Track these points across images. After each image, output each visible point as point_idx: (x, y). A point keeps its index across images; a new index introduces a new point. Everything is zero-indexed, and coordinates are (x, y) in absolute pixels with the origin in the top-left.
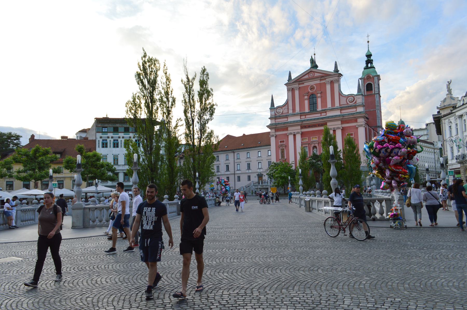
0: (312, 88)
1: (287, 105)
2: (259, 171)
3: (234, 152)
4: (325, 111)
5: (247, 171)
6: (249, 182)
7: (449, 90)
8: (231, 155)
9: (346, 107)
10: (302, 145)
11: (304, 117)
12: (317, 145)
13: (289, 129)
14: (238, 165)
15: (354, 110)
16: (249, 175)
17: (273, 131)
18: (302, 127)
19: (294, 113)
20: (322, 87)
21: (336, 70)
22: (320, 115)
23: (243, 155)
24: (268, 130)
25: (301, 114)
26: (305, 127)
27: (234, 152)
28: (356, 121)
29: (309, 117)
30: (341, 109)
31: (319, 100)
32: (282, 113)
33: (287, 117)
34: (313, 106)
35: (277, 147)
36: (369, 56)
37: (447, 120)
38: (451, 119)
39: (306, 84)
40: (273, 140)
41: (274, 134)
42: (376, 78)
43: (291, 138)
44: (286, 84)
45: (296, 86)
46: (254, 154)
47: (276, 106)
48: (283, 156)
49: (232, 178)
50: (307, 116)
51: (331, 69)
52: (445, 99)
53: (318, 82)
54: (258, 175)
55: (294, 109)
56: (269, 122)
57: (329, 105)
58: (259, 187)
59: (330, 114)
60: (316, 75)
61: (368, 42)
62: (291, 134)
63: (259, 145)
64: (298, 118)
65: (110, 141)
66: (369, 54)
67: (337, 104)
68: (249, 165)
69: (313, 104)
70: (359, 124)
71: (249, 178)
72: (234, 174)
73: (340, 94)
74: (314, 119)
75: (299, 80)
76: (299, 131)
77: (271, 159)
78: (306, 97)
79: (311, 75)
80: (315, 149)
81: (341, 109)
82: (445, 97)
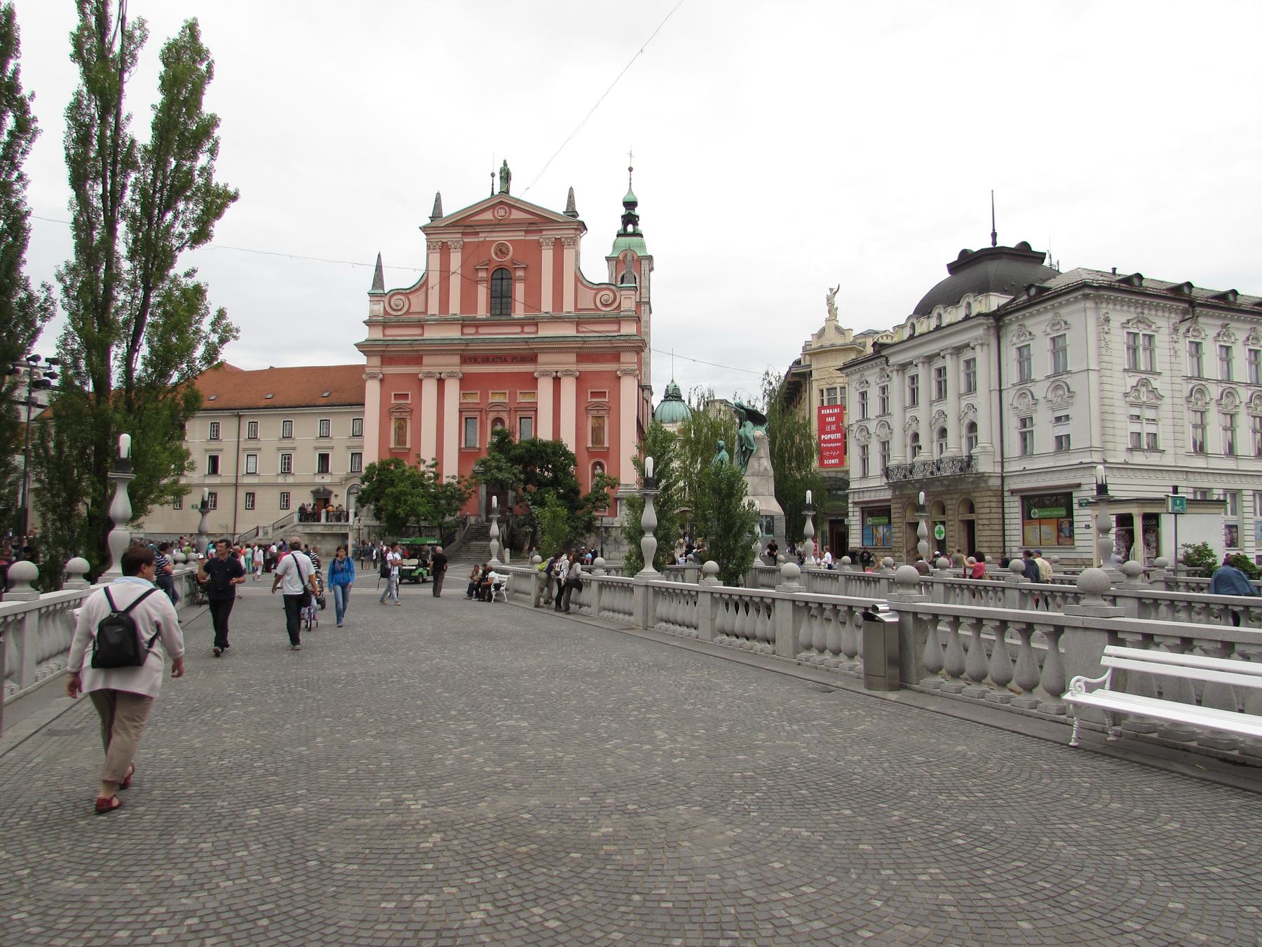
0: (502, 251)
2: (318, 479)
3: (240, 417)
4: (534, 322)
5: (281, 480)
6: (286, 513)
7: (832, 310)
8: (228, 429)
10: (461, 412)
11: (472, 330)
12: (504, 416)
13: (426, 360)
14: (252, 459)
15: (615, 327)
16: (285, 490)
17: (376, 361)
18: (467, 359)
19: (444, 316)
21: (572, 212)
22: (518, 330)
23: (270, 430)
24: (361, 360)
25: (464, 323)
27: (240, 417)
28: (616, 358)
29: (487, 333)
31: (519, 289)
32: (407, 312)
33: (421, 325)
34: (501, 301)
35: (387, 412)
36: (630, 205)
37: (857, 376)
40: (373, 391)
41: (377, 370)
42: (645, 263)
43: (429, 388)
44: (424, 229)
45: (453, 238)
46: (306, 430)
47: (389, 286)
48: (401, 439)
50: (481, 330)
51: (559, 207)
52: (823, 330)
53: (520, 236)
54: (315, 493)
56: (364, 334)
58: (319, 530)
59: (546, 331)
60: (516, 215)
61: (631, 169)
62: (429, 375)
63: (324, 401)
64: (454, 333)
66: (630, 199)
67: (568, 307)
68: (287, 461)
69: (502, 297)
70: (623, 367)
71: (285, 500)
72: (236, 485)
73: (579, 278)
74: (503, 341)
75: (466, 223)
76: (457, 369)
77: (362, 447)
78: (482, 274)
79: (502, 212)
81: (579, 322)
82: (823, 324)
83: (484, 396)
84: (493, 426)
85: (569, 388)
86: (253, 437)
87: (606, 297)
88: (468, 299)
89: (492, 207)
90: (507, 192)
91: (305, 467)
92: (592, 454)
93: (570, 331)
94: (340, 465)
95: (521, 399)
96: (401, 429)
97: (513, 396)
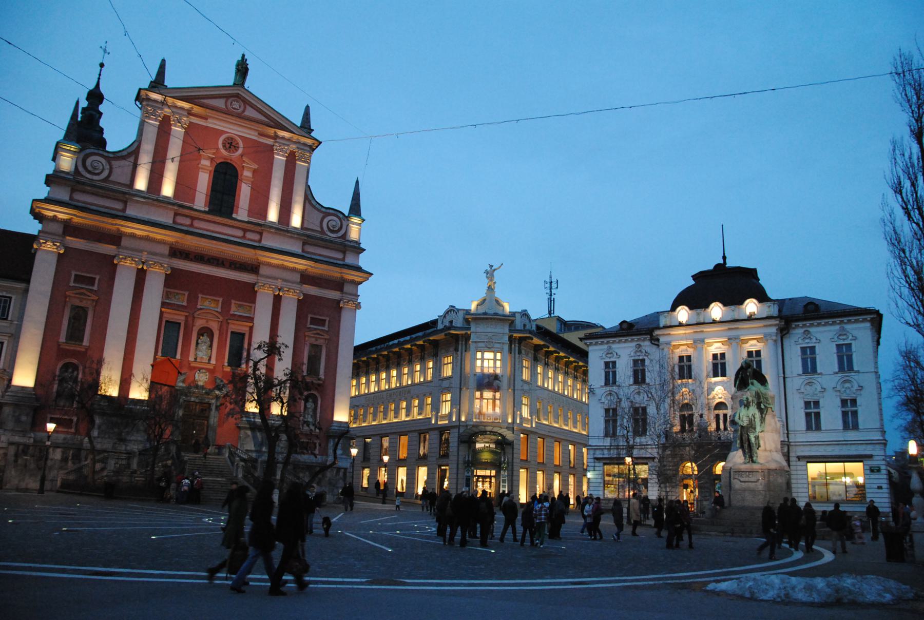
0: (231, 144)
1: (132, 159)
9: (316, 238)
11: (187, 221)
12: (214, 326)
19: (155, 197)
20: (264, 154)
22: (240, 233)
31: (245, 192)
32: (106, 180)
37: (605, 347)
38: (614, 346)
39: (212, 124)
48: (75, 334)
50: (197, 223)
53: (253, 135)
60: (250, 112)
73: (309, 198)
79: (236, 105)
80: (205, 338)
84: (198, 338)
87: (334, 223)
88: (184, 184)
89: (227, 97)
90: (243, 84)
95: (234, 310)
97: (226, 306)
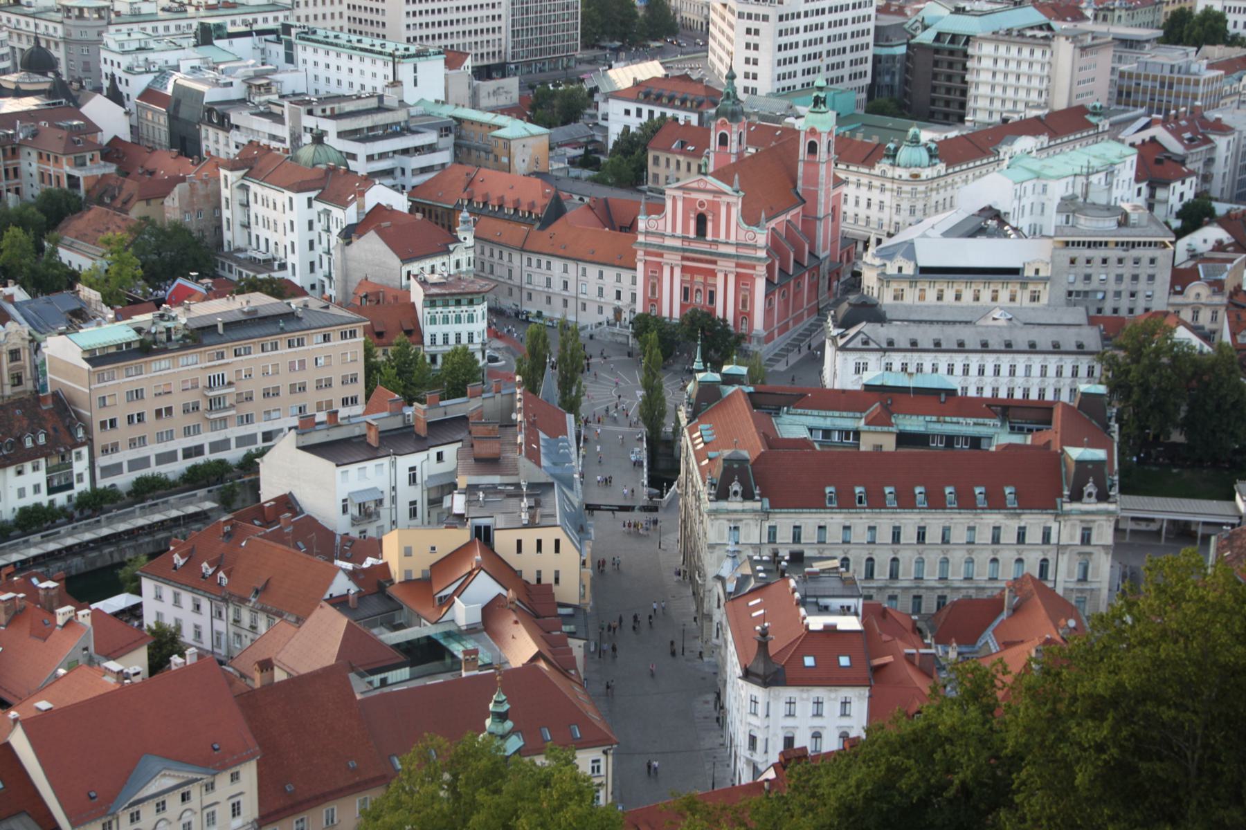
0: (702, 204)
8: (572, 266)
18: (684, 258)
26: (688, 259)
29: (695, 246)
30: (738, 245)
31: (710, 225)
35: (646, 279)
40: (640, 266)
45: (679, 193)
48: (653, 293)
49: (571, 303)
55: (674, 228)
57: (722, 237)
65: (439, 317)
67: (733, 239)
71: (601, 310)
83: (692, 278)
85: (731, 279)
86: (584, 274)
88: (685, 227)
91: (610, 296)
92: (742, 313)
93: (731, 250)
94: (626, 297)
96: (653, 287)
97: (705, 279)
